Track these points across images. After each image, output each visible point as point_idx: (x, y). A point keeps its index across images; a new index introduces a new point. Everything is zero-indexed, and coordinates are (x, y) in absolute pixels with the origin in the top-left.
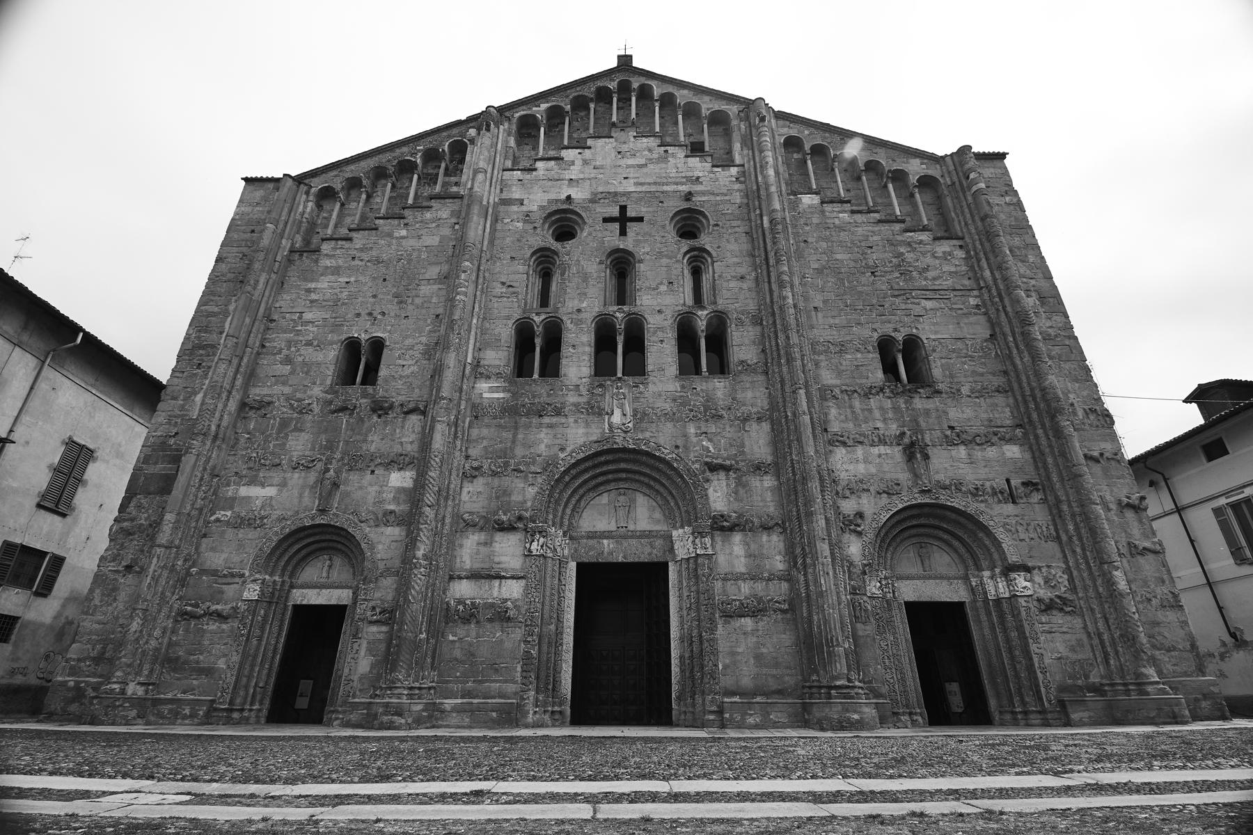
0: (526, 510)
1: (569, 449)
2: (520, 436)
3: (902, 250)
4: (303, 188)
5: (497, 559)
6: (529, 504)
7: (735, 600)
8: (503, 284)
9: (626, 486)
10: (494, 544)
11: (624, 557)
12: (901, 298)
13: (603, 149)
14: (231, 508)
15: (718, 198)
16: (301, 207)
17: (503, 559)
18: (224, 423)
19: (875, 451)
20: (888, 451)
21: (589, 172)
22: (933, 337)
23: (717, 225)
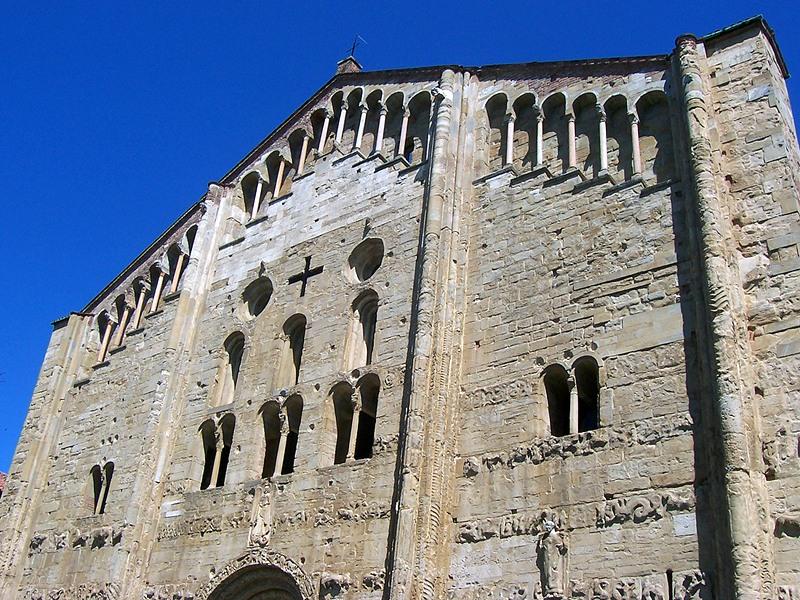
2: (185, 557)
3: (596, 223)
4: (87, 319)
8: (199, 384)
12: (582, 300)
13: (302, 189)
15: (398, 216)
16: (84, 339)
18: (15, 562)
19: (507, 543)
20: (523, 543)
22: (611, 354)
23: (391, 254)
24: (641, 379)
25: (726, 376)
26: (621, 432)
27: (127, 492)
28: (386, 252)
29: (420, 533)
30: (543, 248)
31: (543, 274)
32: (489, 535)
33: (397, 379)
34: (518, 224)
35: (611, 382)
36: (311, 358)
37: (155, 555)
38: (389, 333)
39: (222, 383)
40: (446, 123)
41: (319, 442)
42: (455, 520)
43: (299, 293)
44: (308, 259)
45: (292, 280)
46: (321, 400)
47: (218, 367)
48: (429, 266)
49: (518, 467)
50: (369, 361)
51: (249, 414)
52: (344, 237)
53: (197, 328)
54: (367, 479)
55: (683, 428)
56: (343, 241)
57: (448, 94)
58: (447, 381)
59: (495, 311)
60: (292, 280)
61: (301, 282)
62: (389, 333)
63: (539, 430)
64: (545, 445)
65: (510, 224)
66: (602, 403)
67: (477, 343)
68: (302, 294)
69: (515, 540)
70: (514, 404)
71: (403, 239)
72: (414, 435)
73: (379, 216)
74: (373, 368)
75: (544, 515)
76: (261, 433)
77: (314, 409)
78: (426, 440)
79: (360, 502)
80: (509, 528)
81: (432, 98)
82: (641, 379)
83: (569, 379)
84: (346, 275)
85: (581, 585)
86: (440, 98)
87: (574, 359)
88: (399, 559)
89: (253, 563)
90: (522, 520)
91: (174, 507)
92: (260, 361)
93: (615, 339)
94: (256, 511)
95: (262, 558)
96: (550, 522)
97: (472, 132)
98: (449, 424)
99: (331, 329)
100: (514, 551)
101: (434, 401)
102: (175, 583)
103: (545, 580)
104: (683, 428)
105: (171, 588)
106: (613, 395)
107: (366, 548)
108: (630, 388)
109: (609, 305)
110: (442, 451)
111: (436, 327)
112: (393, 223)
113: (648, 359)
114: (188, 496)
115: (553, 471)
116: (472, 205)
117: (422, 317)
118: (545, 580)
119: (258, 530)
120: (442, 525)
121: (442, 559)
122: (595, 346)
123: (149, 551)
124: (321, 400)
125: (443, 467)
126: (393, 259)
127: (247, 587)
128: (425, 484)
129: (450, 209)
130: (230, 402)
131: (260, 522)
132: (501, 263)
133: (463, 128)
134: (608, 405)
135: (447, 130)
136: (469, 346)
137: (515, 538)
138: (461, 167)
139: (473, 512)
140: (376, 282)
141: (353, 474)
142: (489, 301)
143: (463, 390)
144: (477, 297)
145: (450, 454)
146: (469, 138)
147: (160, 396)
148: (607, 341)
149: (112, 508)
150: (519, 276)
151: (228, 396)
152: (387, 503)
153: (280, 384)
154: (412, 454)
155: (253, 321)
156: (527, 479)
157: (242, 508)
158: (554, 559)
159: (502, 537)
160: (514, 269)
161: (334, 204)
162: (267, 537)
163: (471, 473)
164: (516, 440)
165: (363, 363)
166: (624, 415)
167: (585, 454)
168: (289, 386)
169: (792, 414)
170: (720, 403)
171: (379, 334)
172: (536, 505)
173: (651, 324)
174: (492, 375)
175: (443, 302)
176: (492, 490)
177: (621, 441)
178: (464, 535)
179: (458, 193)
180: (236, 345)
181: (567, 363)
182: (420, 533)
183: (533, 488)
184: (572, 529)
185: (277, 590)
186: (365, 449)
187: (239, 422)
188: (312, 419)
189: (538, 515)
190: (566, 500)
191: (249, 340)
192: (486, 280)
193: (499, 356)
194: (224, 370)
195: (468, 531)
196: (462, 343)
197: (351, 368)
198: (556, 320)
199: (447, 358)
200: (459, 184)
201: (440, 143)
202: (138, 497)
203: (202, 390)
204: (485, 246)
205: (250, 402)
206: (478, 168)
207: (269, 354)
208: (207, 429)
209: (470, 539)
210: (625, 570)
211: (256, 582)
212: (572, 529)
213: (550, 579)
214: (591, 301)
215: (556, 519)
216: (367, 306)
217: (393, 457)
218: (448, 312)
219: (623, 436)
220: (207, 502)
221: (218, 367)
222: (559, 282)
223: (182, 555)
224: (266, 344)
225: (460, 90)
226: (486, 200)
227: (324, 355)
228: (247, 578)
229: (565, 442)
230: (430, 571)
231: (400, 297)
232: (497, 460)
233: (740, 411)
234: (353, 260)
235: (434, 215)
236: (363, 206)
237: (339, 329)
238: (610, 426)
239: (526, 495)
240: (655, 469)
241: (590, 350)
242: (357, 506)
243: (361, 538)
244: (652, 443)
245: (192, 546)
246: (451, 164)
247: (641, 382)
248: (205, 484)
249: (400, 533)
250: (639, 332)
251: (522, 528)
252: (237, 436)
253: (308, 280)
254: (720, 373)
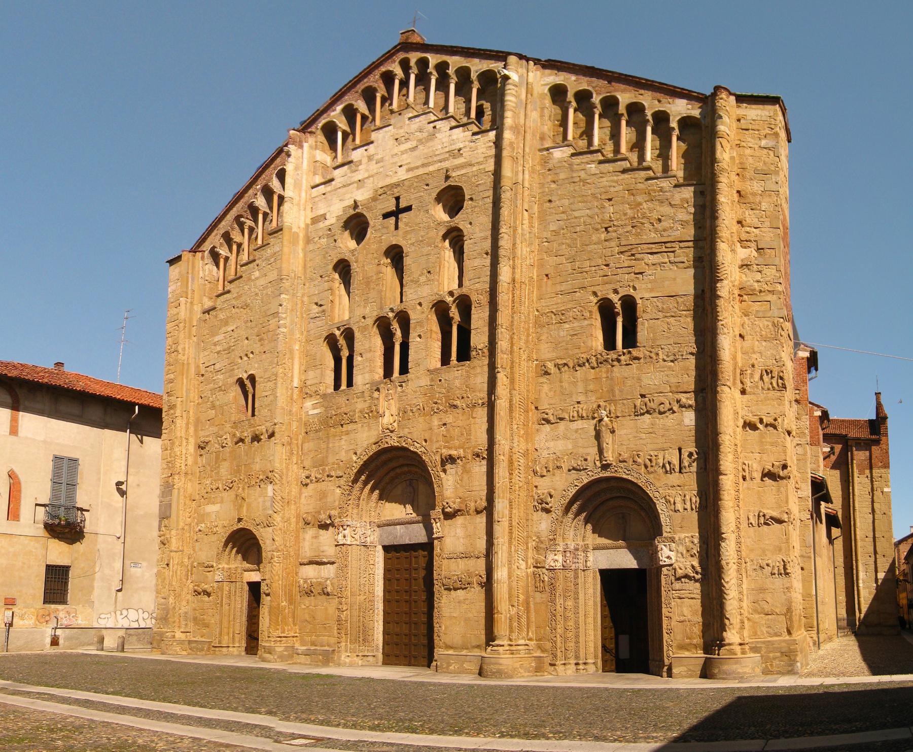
0: (335, 509)
1: (358, 453)
6: (337, 503)
7: (454, 575)
8: (316, 304)
11: (410, 540)
12: (627, 254)
21: (374, 167)
23: (471, 199)
24: (666, 317)
25: (722, 323)
26: (651, 352)
27: (271, 398)
28: (467, 197)
29: (511, 417)
30: (597, 210)
31: (597, 230)
32: (561, 419)
33: (485, 299)
34: (577, 188)
35: (645, 316)
36: (412, 281)
37: (306, 446)
38: (477, 262)
39: (337, 302)
40: (513, 99)
41: (427, 348)
42: (536, 408)
43: (393, 227)
44: (398, 199)
45: (386, 216)
46: (424, 315)
47: (331, 289)
48: (505, 212)
49: (581, 372)
50: (460, 285)
51: (365, 328)
52: (427, 182)
53: (305, 256)
54: (469, 377)
55: (692, 354)
56: (427, 185)
57: (514, 76)
58: (525, 304)
59: (560, 253)
60: (386, 216)
61: (393, 219)
62: (477, 262)
63: (594, 344)
64: (599, 356)
65: (571, 187)
66: (639, 329)
67: (547, 275)
68: (397, 228)
69: (580, 424)
70: (576, 324)
71: (481, 188)
72: (502, 344)
73: (462, 166)
74: (464, 290)
75: (599, 406)
76: (378, 343)
77: (420, 323)
78: (512, 347)
79: (465, 395)
80: (575, 414)
81: (498, 76)
82: (666, 317)
83: (616, 310)
84: (433, 213)
85: (625, 456)
86: (506, 78)
87: (620, 296)
88: (498, 437)
89: (386, 446)
90: (584, 409)
91: (314, 407)
92: (368, 284)
93: (649, 286)
94: (382, 405)
95: (393, 442)
96: (603, 412)
97: (536, 110)
98: (528, 335)
99: (425, 258)
100: (580, 431)
101: (516, 318)
102: (327, 465)
103: (601, 451)
104: (692, 354)
105: (323, 470)
106: (646, 325)
107: (473, 430)
108: (659, 322)
109: (646, 261)
110: (524, 357)
111: (514, 261)
112: (471, 174)
113: (671, 303)
114: (324, 396)
115: (604, 375)
116: (538, 168)
117: (502, 252)
118: (601, 451)
119: (387, 420)
120: (528, 412)
121: (528, 437)
122: (635, 289)
123: (300, 442)
124: (424, 315)
125: (525, 368)
126: (474, 204)
127: (385, 463)
128: (512, 381)
129: (520, 168)
130: (347, 318)
131: (387, 414)
132: (564, 216)
133: (529, 106)
134: (643, 333)
135: (514, 105)
136: (540, 277)
137: (580, 422)
138: (528, 137)
139: (549, 401)
140: (460, 220)
141: (457, 373)
142: (555, 245)
143: (537, 311)
144: (545, 240)
145: (529, 359)
146: (534, 115)
147: (284, 316)
148: (644, 286)
149: (261, 411)
150: (578, 229)
151: (344, 313)
152: (484, 394)
153: (388, 304)
154: (502, 359)
155: (355, 250)
156: (587, 380)
157: (371, 403)
158: (607, 438)
159: (571, 421)
160: (574, 223)
161: (416, 153)
162: (395, 424)
163: (547, 373)
164: (577, 351)
165: (455, 286)
166: (654, 340)
167: (627, 365)
168: (397, 306)
169: (758, 354)
170: (717, 340)
171: (467, 263)
172: (594, 398)
173: (675, 279)
174: (559, 301)
175: (518, 241)
176: (562, 386)
177: (651, 358)
178: (544, 419)
179: (527, 157)
180: (343, 269)
181: (615, 298)
182: (511, 417)
183: (591, 387)
184: (618, 417)
185: (408, 465)
186: (465, 354)
187: (357, 335)
188: (419, 331)
189: (595, 406)
190: (614, 396)
191: (354, 266)
192: (553, 227)
193: (564, 287)
194: (337, 292)
195: (546, 416)
196: (535, 274)
197: (446, 289)
198: (607, 265)
199: (523, 286)
200: (527, 150)
201: (508, 114)
202: (282, 400)
203: (321, 309)
204: (550, 201)
205: (364, 318)
206: (542, 139)
207: (374, 278)
208: (331, 341)
209: (548, 421)
210: (655, 446)
211: (390, 460)
212: (618, 417)
213: (605, 451)
214: (633, 255)
215: (608, 409)
216: (455, 238)
217: (486, 361)
218: (523, 250)
219: (653, 355)
220: (341, 399)
221: (331, 289)
222: (609, 238)
223: (328, 443)
224: (371, 269)
225: (525, 75)
226: (550, 166)
227: (423, 279)
228: (384, 457)
229: (613, 355)
230: (520, 446)
231: (482, 235)
232: (565, 364)
233: (729, 347)
234: (439, 199)
235: (507, 171)
236: (442, 157)
237: (432, 258)
238: (644, 347)
239: (586, 392)
240: (674, 380)
241: (632, 290)
242: (463, 398)
243: (468, 422)
244: (672, 361)
245: (335, 436)
246: (519, 133)
247: (666, 319)
248: (337, 386)
249: (497, 419)
250: (667, 283)
251: (584, 415)
252: (357, 346)
253: (400, 216)
254: (719, 320)
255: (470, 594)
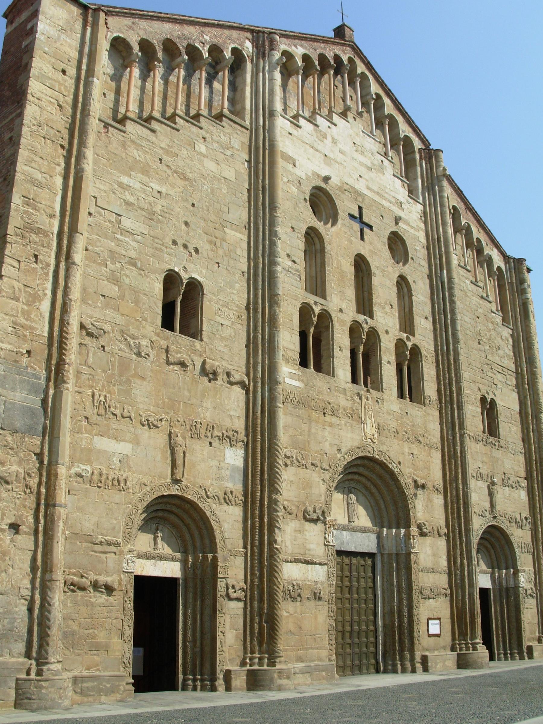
5: (308, 547)
9: (354, 485)
10: (306, 533)
11: (355, 547)
14: (89, 461)
17: (312, 546)
255: (438, 603)
